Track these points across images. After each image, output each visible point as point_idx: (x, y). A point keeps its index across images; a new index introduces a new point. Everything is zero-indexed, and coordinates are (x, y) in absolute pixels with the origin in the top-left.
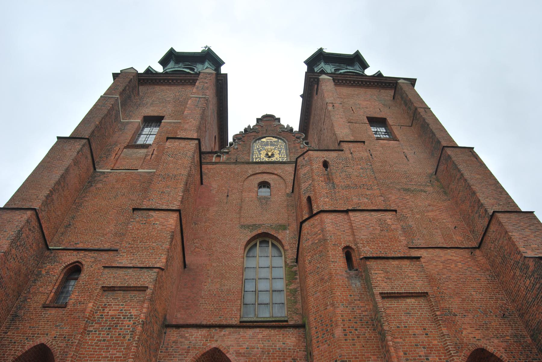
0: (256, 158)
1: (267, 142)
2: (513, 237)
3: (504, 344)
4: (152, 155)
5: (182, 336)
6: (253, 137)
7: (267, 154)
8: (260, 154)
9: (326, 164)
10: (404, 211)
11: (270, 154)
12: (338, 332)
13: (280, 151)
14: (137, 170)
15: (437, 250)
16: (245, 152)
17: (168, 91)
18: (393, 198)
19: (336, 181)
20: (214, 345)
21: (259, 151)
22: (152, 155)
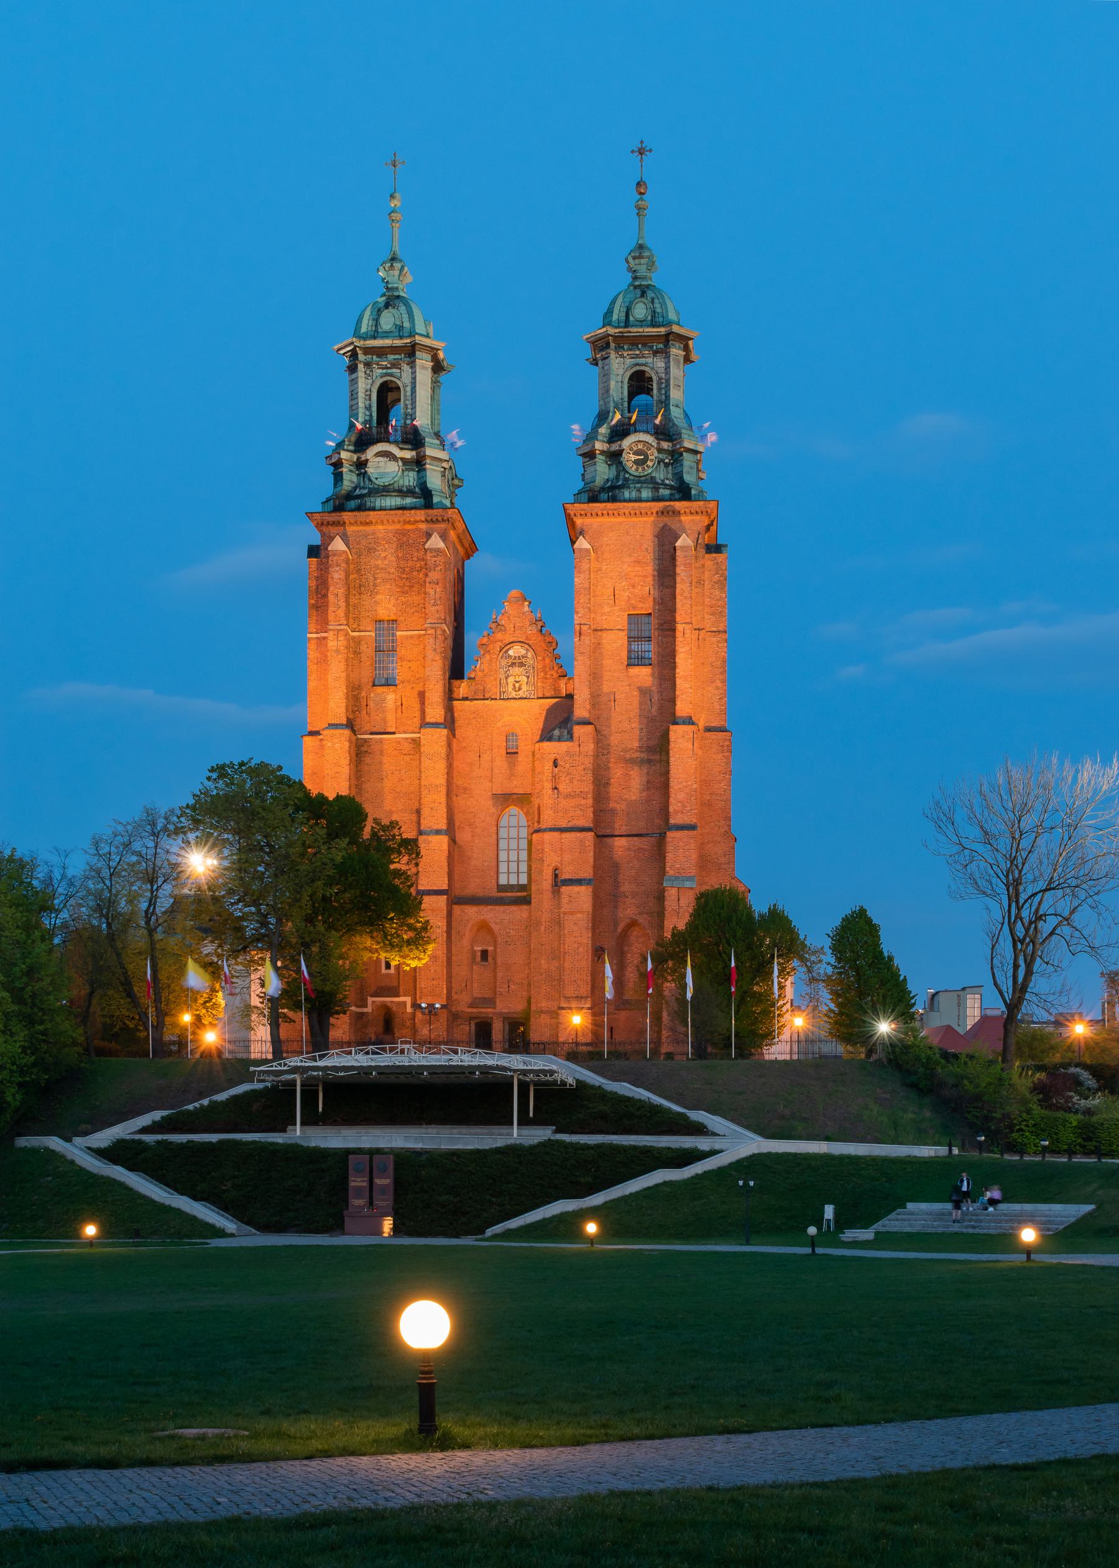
0: (504, 693)
1: (515, 657)
2: (667, 858)
3: (651, 918)
4: (402, 705)
5: (463, 912)
6: (500, 644)
7: (514, 686)
8: (507, 684)
9: (555, 764)
10: (624, 791)
11: (517, 685)
12: (542, 928)
13: (528, 677)
14: (394, 733)
15: (635, 838)
16: (492, 678)
17: (387, 546)
18: (618, 774)
19: (561, 787)
20: (482, 918)
21: (507, 678)
22: (402, 705)
